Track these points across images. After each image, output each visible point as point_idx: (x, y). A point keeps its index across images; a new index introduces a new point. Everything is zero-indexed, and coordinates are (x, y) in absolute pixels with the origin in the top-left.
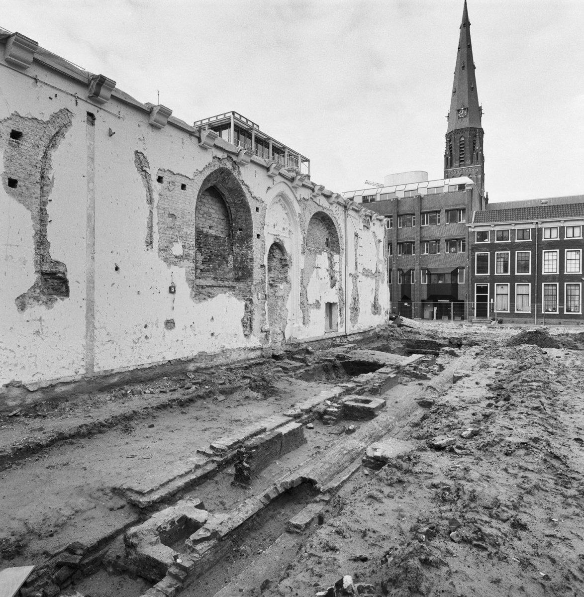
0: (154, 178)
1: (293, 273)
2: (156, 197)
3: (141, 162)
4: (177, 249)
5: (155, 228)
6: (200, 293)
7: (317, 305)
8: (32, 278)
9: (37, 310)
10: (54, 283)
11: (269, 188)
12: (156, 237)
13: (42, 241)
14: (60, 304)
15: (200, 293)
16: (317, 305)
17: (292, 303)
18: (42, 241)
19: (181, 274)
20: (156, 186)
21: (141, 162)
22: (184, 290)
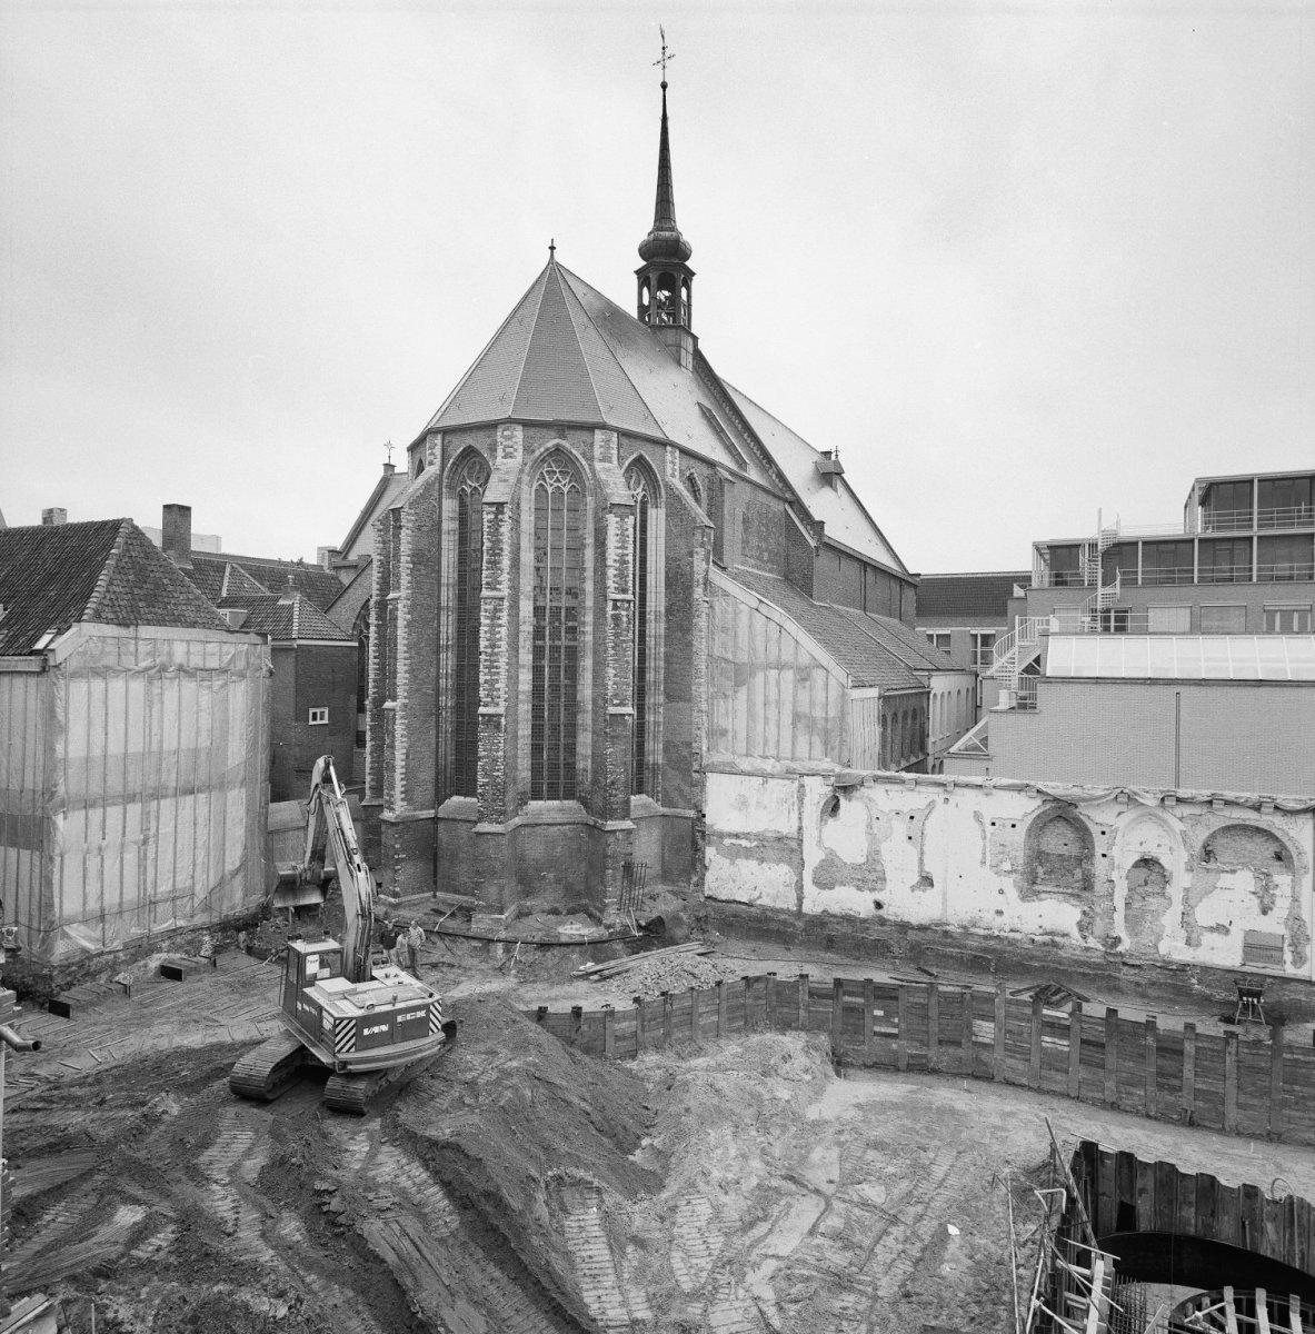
0: (987, 823)
1: (1175, 891)
2: (989, 836)
3: (977, 816)
4: (1007, 866)
5: (988, 854)
6: (1024, 898)
7: (1222, 929)
8: (916, 879)
9: (918, 893)
10: (927, 881)
11: (1119, 814)
12: (988, 858)
13: (921, 861)
14: (929, 891)
15: (1024, 898)
16: (1222, 929)
17: (1170, 919)
18: (921, 861)
19: (1008, 883)
20: (990, 829)
21: (977, 816)
22: (1012, 894)
